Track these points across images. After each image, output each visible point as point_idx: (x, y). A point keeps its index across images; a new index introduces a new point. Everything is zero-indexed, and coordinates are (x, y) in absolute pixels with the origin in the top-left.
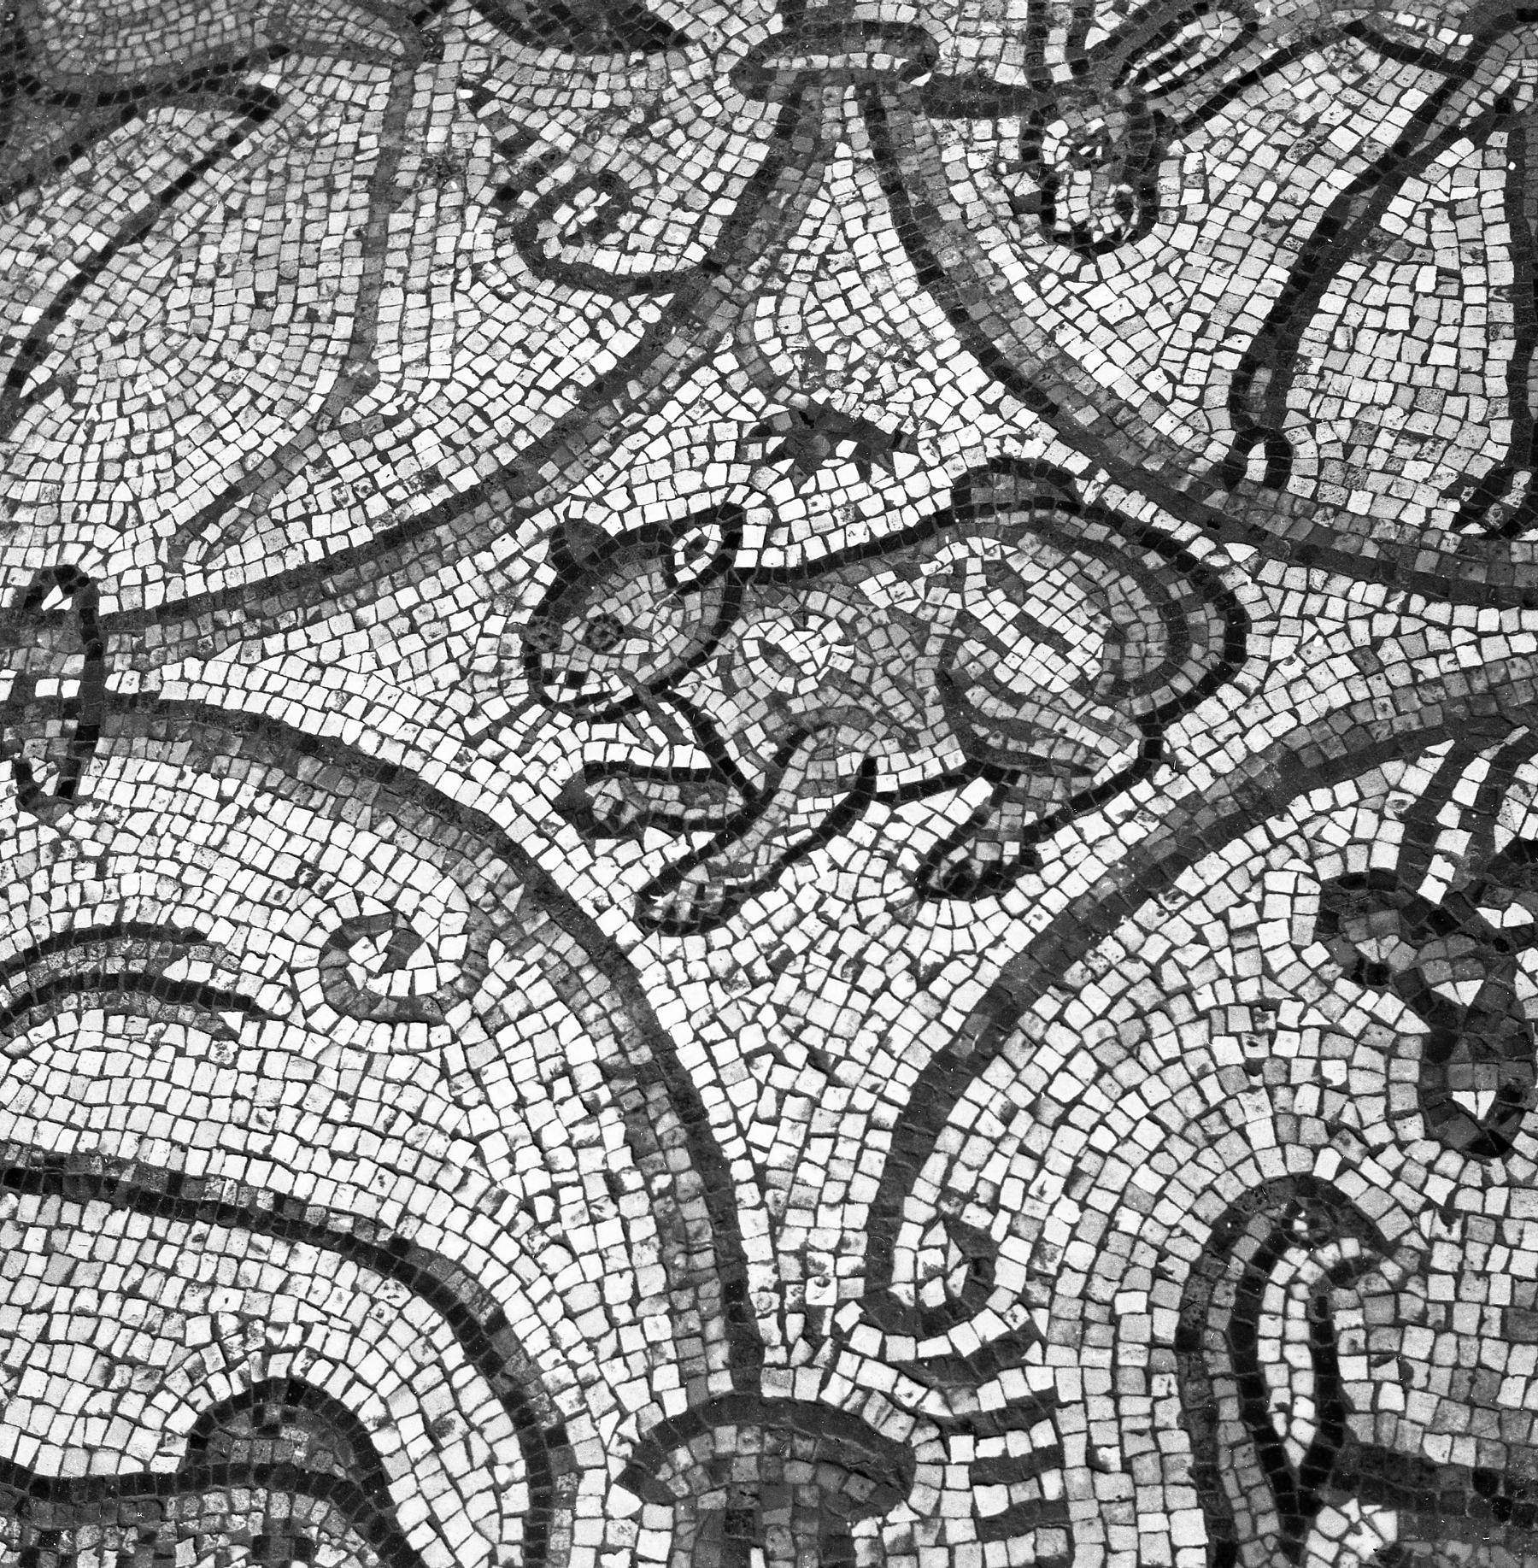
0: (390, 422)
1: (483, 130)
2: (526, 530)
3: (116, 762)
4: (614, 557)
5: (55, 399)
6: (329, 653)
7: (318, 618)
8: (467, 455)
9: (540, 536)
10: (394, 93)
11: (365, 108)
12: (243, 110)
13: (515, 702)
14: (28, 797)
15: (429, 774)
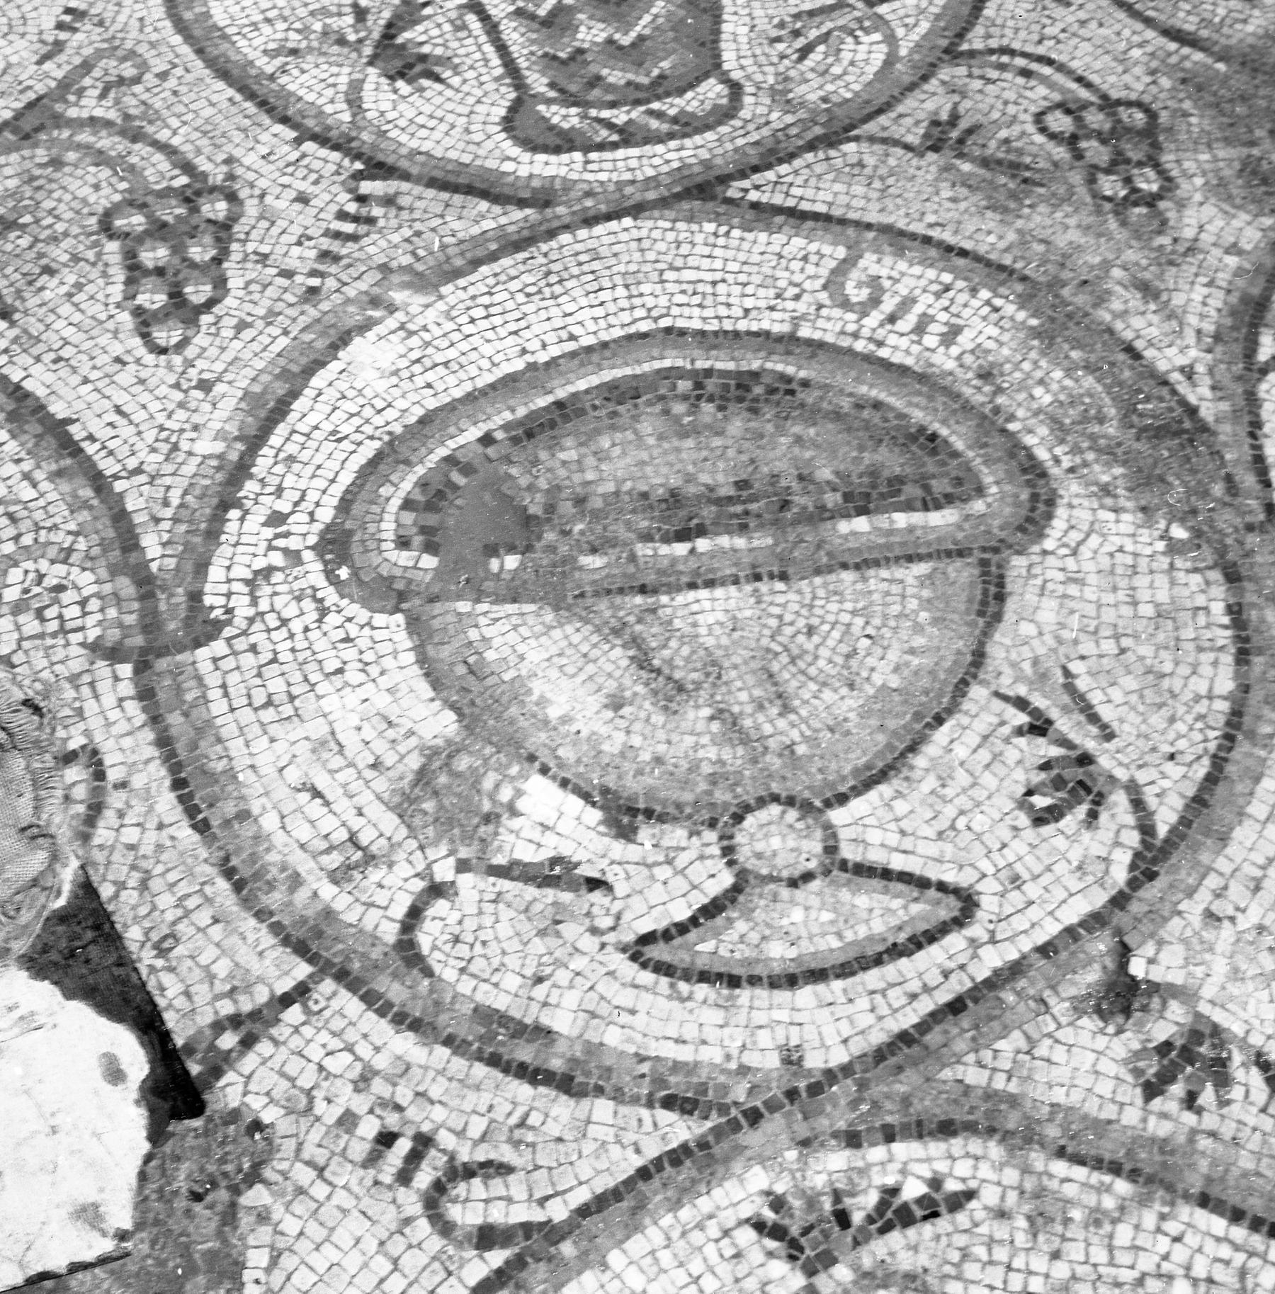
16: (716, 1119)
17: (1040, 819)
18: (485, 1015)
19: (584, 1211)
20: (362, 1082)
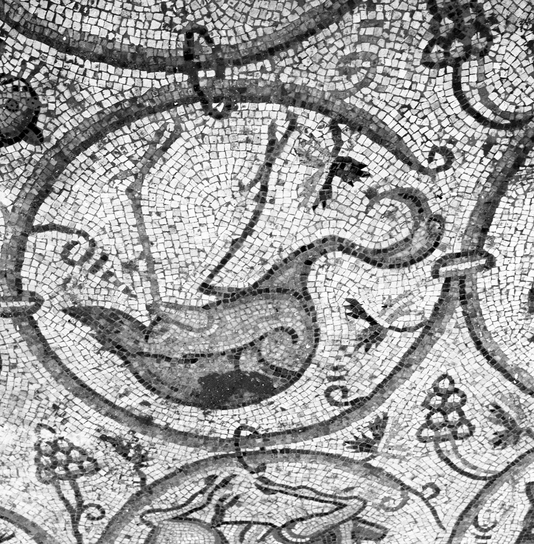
0: (115, 177)
1: (121, 280)
2: (54, 141)
3: (173, 47)
4: (19, 133)
5: (246, 182)
6: (107, 93)
7: (117, 105)
8: (84, 166)
9: (49, 139)
10: (158, 294)
11: (167, 288)
12: (211, 287)
13: (33, 80)
14: (203, 32)
15: (54, 52)
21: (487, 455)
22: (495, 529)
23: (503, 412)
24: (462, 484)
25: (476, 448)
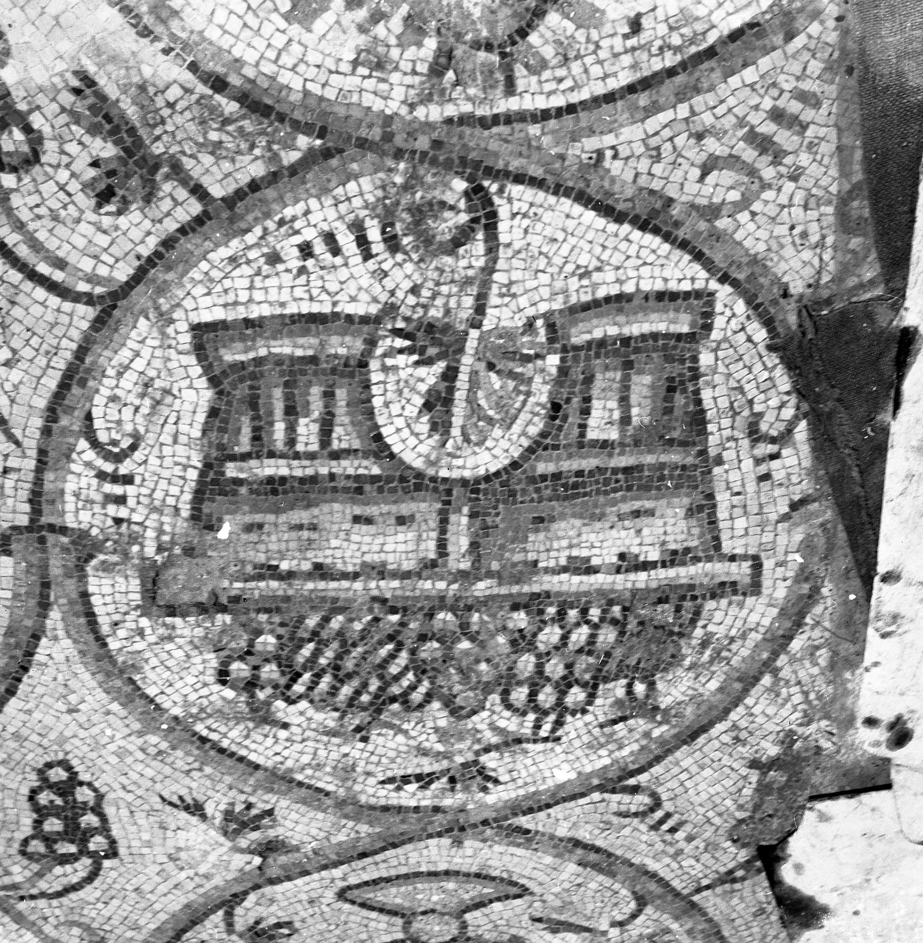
16: (506, 825)
17: (289, 924)
18: (612, 874)
19: (583, 795)
20: (680, 852)
21: (83, 227)
22: (138, 455)
23: (103, 98)
24: (36, 310)
25: (56, 205)
